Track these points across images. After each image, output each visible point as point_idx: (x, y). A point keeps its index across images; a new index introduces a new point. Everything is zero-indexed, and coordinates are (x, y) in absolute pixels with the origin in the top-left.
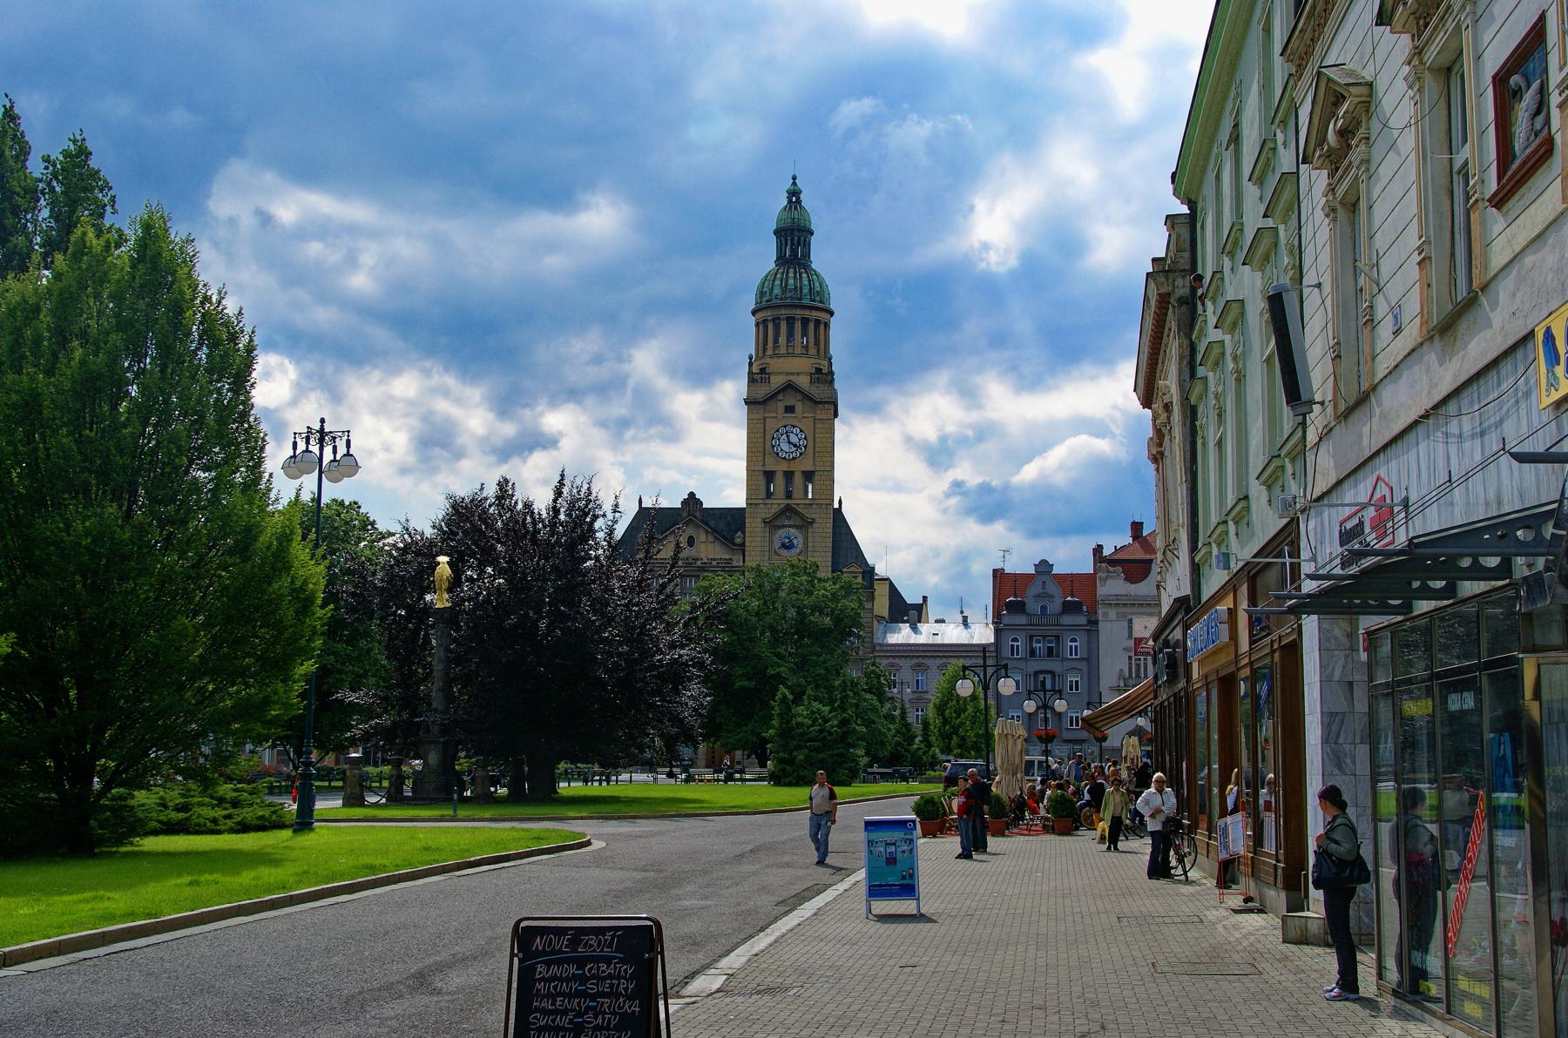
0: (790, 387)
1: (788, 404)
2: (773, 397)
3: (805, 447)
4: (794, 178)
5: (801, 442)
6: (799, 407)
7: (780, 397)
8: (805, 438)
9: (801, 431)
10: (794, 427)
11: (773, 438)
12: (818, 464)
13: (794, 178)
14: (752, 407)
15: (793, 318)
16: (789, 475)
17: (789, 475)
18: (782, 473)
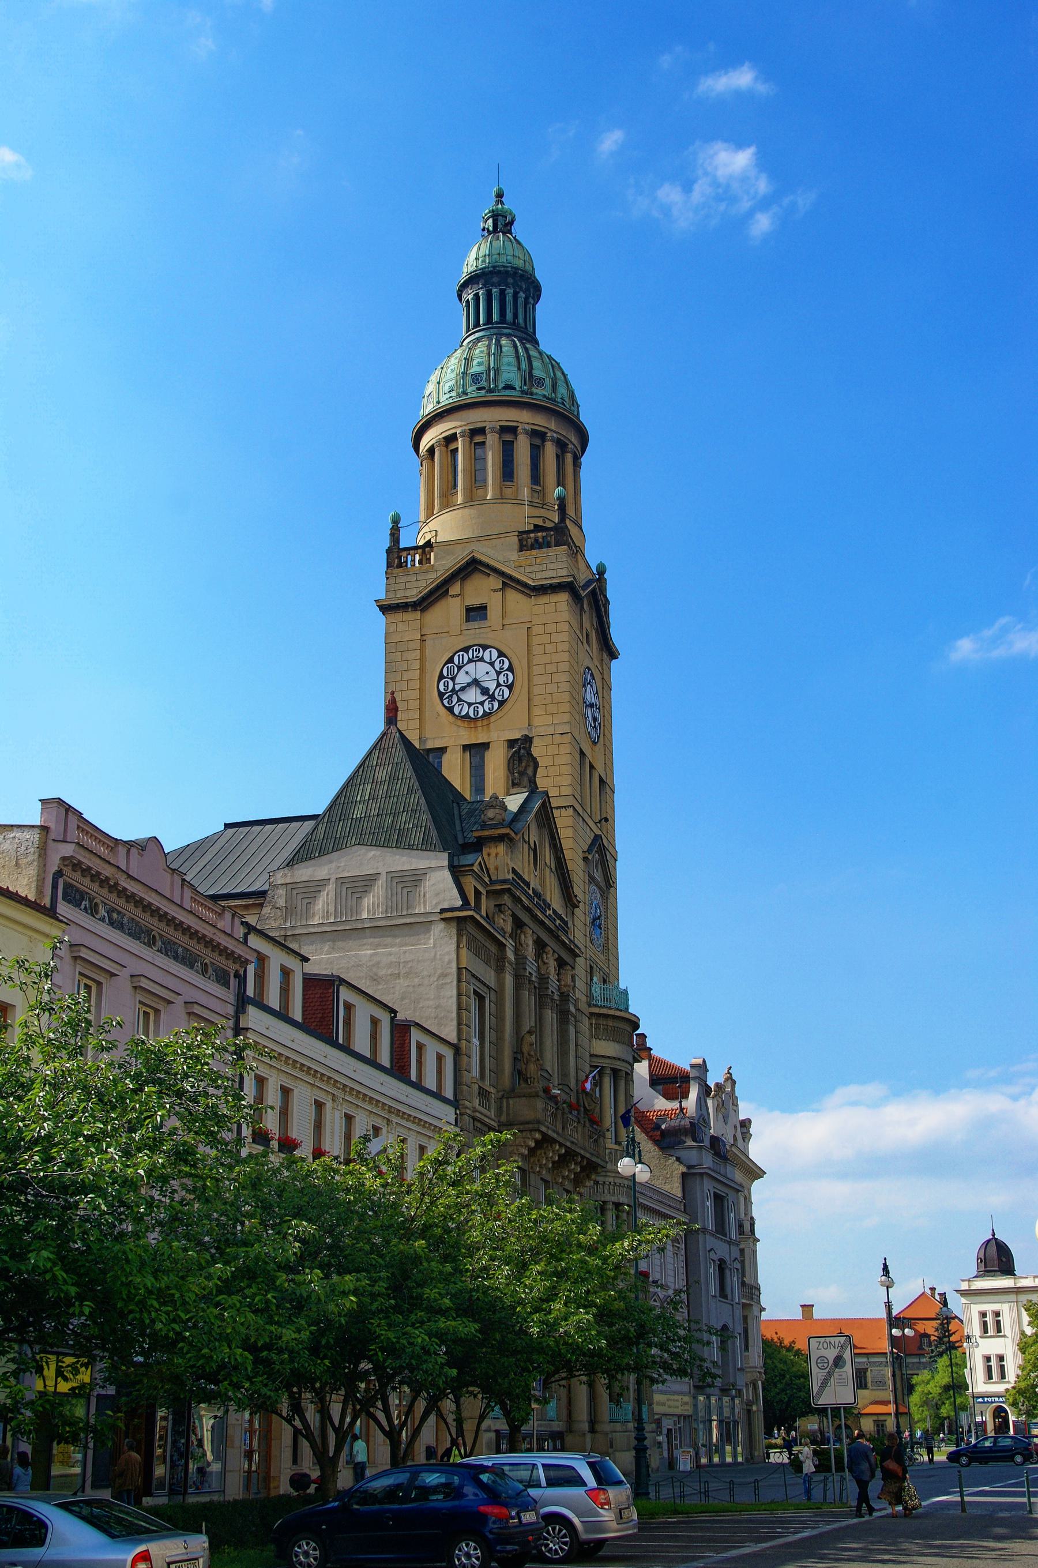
0: (472, 567)
1: (473, 601)
2: (438, 593)
3: (510, 687)
4: (500, 195)
5: (502, 679)
6: (494, 603)
7: (455, 589)
8: (511, 669)
9: (501, 654)
10: (485, 647)
11: (441, 677)
12: (536, 722)
13: (500, 195)
14: (398, 616)
15: (481, 431)
16: (477, 751)
17: (477, 751)
18: (460, 749)
